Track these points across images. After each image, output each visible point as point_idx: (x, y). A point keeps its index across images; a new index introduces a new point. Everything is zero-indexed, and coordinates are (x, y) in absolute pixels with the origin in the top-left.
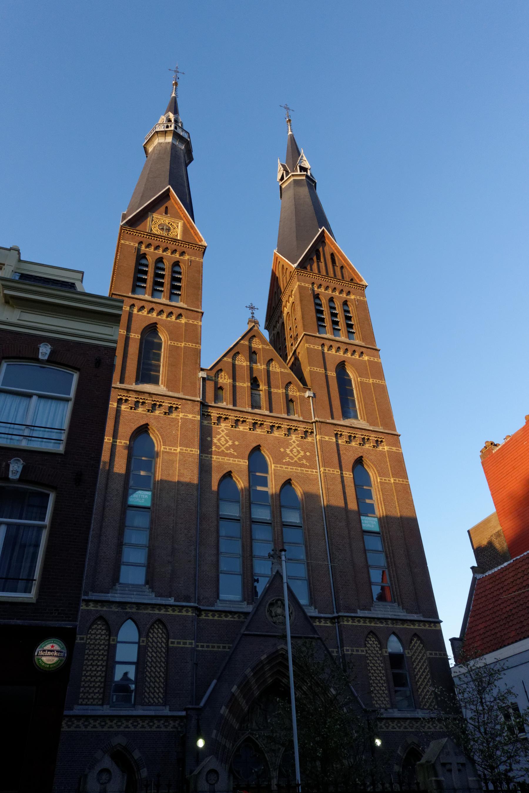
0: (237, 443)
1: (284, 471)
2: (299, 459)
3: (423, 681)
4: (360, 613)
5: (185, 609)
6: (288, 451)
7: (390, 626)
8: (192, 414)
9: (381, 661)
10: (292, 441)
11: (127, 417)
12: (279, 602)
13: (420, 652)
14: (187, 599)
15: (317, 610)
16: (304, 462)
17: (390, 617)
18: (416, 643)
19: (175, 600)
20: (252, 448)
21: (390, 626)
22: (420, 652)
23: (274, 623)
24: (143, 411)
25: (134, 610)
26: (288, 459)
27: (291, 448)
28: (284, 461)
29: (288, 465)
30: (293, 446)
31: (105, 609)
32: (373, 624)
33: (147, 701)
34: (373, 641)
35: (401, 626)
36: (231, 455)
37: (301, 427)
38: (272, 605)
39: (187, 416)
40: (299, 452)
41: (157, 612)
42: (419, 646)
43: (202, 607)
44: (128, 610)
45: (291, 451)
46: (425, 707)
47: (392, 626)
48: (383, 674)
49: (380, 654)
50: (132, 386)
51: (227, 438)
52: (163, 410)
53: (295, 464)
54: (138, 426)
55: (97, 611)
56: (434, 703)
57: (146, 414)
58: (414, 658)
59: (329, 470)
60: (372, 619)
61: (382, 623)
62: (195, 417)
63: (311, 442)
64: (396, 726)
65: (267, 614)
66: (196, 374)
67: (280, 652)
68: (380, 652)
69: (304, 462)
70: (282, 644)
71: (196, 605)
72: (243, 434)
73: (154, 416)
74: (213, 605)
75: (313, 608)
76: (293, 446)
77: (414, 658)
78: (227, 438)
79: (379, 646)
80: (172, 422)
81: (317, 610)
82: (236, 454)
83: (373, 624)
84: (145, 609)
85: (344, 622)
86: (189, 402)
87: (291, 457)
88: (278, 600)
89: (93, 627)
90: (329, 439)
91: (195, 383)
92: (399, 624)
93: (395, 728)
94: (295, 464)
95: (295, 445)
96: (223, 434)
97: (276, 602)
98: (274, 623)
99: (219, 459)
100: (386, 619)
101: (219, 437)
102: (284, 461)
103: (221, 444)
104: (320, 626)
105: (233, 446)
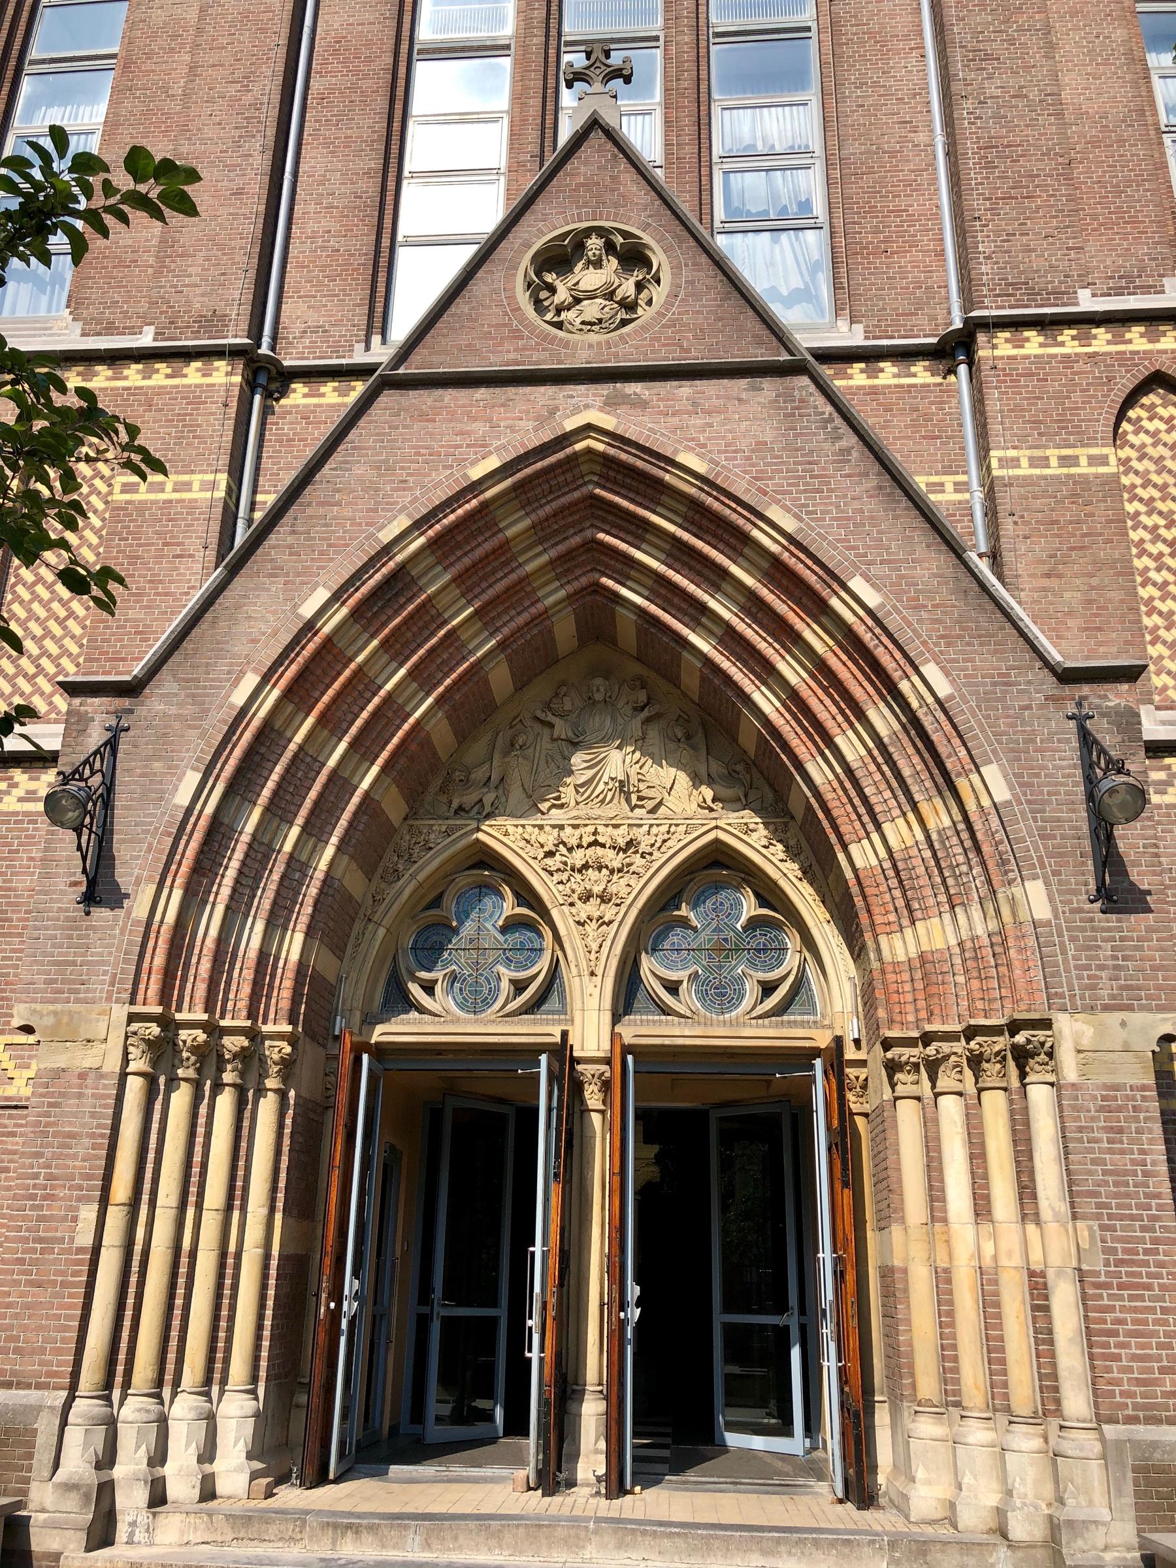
12: (594, 244)
38: (559, 258)
65: (523, 299)
67: (578, 447)
70: (587, 407)
85: (994, 347)
88: (588, 232)
104: (874, 391)
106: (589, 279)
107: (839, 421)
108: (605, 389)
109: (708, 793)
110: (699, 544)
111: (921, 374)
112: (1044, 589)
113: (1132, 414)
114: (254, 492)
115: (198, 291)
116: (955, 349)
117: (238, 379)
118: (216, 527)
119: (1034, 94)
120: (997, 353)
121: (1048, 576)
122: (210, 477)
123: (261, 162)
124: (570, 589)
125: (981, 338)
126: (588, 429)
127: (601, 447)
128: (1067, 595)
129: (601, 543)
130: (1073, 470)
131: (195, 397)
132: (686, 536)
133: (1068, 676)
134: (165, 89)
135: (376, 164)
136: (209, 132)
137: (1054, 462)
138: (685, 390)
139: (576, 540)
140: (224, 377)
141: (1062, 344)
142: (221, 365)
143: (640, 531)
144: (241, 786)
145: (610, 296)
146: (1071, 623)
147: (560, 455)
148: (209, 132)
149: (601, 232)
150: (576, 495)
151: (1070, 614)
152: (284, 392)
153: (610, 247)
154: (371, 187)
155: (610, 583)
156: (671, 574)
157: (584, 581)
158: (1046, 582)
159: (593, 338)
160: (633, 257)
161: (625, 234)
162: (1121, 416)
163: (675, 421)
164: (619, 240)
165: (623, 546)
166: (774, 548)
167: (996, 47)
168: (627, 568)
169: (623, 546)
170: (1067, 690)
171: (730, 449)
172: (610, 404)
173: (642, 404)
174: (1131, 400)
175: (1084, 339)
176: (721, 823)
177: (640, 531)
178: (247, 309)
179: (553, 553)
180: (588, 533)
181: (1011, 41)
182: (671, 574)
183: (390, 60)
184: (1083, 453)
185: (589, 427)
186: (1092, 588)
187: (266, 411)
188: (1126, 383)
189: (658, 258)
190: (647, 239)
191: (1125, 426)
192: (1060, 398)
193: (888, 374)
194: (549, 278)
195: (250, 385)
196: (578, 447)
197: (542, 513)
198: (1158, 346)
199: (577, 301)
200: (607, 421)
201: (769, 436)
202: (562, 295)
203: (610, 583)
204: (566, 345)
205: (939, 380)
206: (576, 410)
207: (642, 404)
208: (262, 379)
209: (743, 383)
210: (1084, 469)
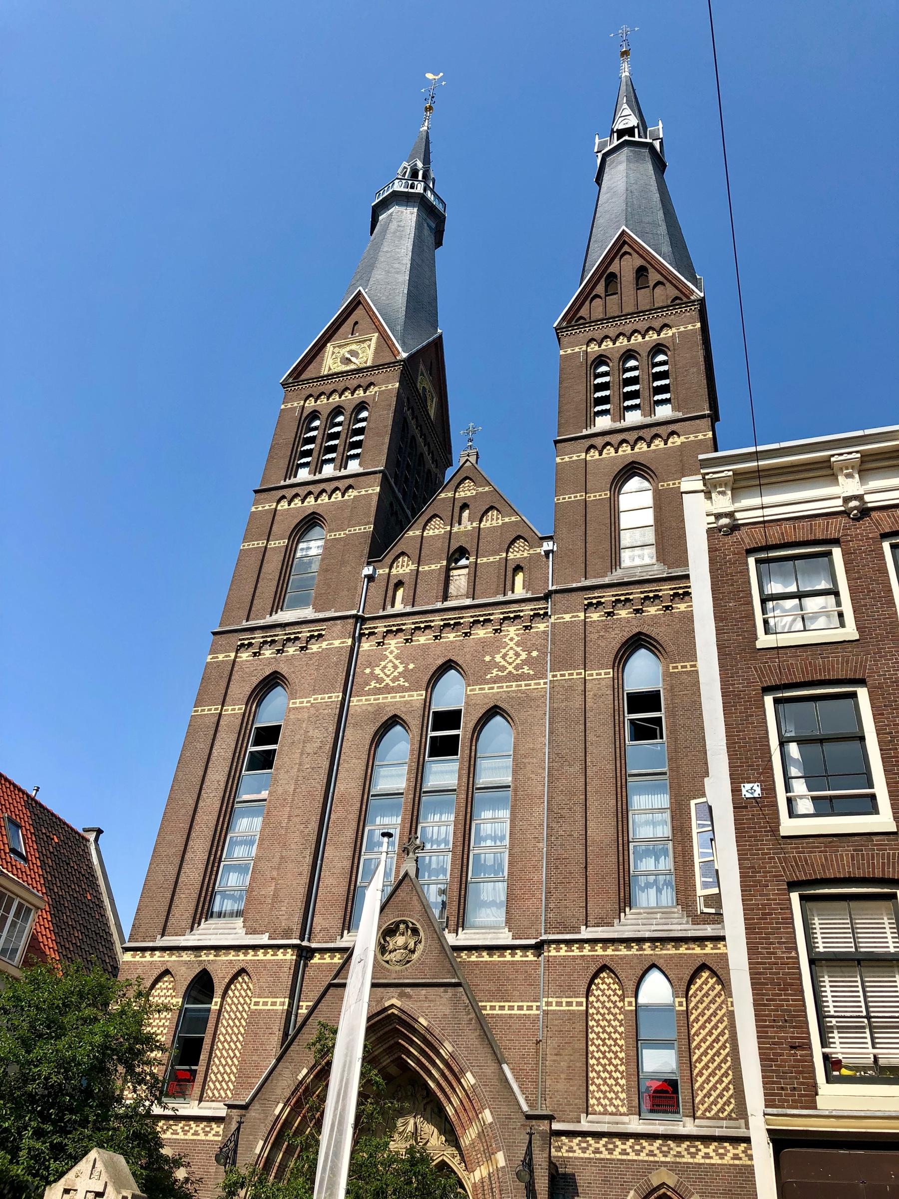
0: (411, 666)
1: (485, 696)
2: (517, 668)
3: (712, 1060)
4: (586, 933)
5: (281, 950)
6: (498, 658)
7: (648, 952)
8: (341, 638)
9: (620, 1021)
10: (509, 637)
11: (247, 670)
12: (402, 926)
13: (713, 1001)
14: (287, 934)
15: (511, 933)
16: (526, 669)
17: (647, 935)
18: (706, 982)
19: (270, 938)
20: (435, 668)
21: (648, 952)
22: (713, 1001)
23: (387, 962)
24: (272, 653)
25: (211, 957)
26: (495, 672)
27: (504, 651)
28: (488, 677)
29: (495, 682)
30: (509, 647)
31: (174, 958)
32: (609, 952)
33: (211, 1095)
34: (608, 985)
35: (673, 951)
36: (403, 689)
37: (525, 611)
39: (331, 644)
40: (517, 655)
41: (698, 950)
42: (712, 988)
43: (314, 945)
44: (204, 958)
45: (504, 657)
46: (721, 1115)
47: (652, 952)
48: (621, 1047)
49: (620, 1009)
50: (262, 621)
51: (397, 662)
52: (298, 644)
53: (511, 677)
54: (261, 678)
55: (164, 962)
56: (732, 1106)
57: (274, 658)
58: (695, 1013)
59: (562, 675)
60: (606, 942)
61: (629, 948)
62: (343, 643)
63: (544, 632)
64: (629, 1150)
66: (360, 573)
67: (390, 1012)
68: (620, 1004)
69: (526, 669)
71: (297, 942)
72: (425, 648)
73: (287, 656)
74: (333, 940)
75: (507, 929)
76: (509, 647)
77: (695, 1013)
78: (397, 662)
79: (620, 993)
80: (311, 660)
81: (511, 933)
82: (407, 684)
83: (609, 952)
84: (226, 955)
85: (549, 951)
86: (339, 622)
87: (503, 666)
89: (157, 986)
90: (573, 617)
91: (356, 589)
92: (669, 946)
93: (628, 1154)
94: (511, 677)
95: (512, 644)
96: (391, 657)
97: (397, 926)
98: (387, 962)
99: (378, 699)
100: (640, 941)
101: (383, 663)
102: (488, 677)
103: (385, 674)
105: (405, 674)
106: (400, 940)
107: (470, 1007)
108: (399, 990)
109: (444, 1139)
110: (427, 1050)
111: (530, 957)
112: (554, 1061)
113: (596, 981)
114: (299, 1001)
115: (284, 917)
116: (538, 948)
117: (294, 957)
118: (283, 1021)
119: (576, 835)
120: (550, 954)
121: (556, 1055)
122: (282, 1000)
123: (309, 860)
124: (391, 1059)
125: (546, 947)
126: (392, 1006)
127: (396, 1012)
128: (562, 1064)
129: (400, 1043)
130: (571, 1008)
131: (279, 964)
132: (423, 1046)
133: (529, 1117)
134: (280, 823)
135: (350, 854)
136: (293, 846)
137: (564, 1004)
138: (423, 991)
139: (392, 1042)
140: (290, 956)
141: (573, 951)
142: (289, 950)
143: (412, 1043)
144: (276, 1145)
145: (406, 948)
146: (563, 1076)
147: (383, 1015)
148: (293, 846)
149: (404, 922)
150: (391, 1027)
151: (562, 1072)
152: (312, 957)
153: (407, 927)
154: (347, 864)
155: (405, 1057)
156: (421, 1058)
157: (396, 1056)
158: (555, 1058)
159: (398, 968)
160: (415, 931)
161: (413, 924)
162: (591, 982)
163: (419, 1004)
164: (411, 925)
165: (407, 1045)
166: (446, 1057)
167: (564, 812)
168: (409, 1054)
169: (407, 1045)
170: (529, 1122)
171: (435, 1017)
172: (401, 996)
173: (409, 997)
174: (596, 975)
175: (581, 949)
176: (445, 1153)
177: (412, 1043)
178: (299, 926)
179: (384, 1047)
180: (396, 1040)
181: (570, 809)
182: (421, 1058)
183: (359, 805)
184: (574, 1000)
185: (393, 1005)
186: (571, 1061)
187: (306, 965)
188: (593, 969)
189: (422, 933)
190: (418, 926)
191: (593, 987)
192: (569, 975)
193: (519, 956)
194: (388, 939)
195: (300, 956)
196: (390, 1012)
197: (379, 1035)
198: (606, 953)
199: (396, 950)
200: (398, 1003)
201: (447, 1012)
202: (391, 947)
203: (405, 1057)
204: (388, 970)
205: (536, 959)
206: (389, 999)
207: (409, 997)
208: (304, 954)
209: (442, 989)
210: (574, 1008)
